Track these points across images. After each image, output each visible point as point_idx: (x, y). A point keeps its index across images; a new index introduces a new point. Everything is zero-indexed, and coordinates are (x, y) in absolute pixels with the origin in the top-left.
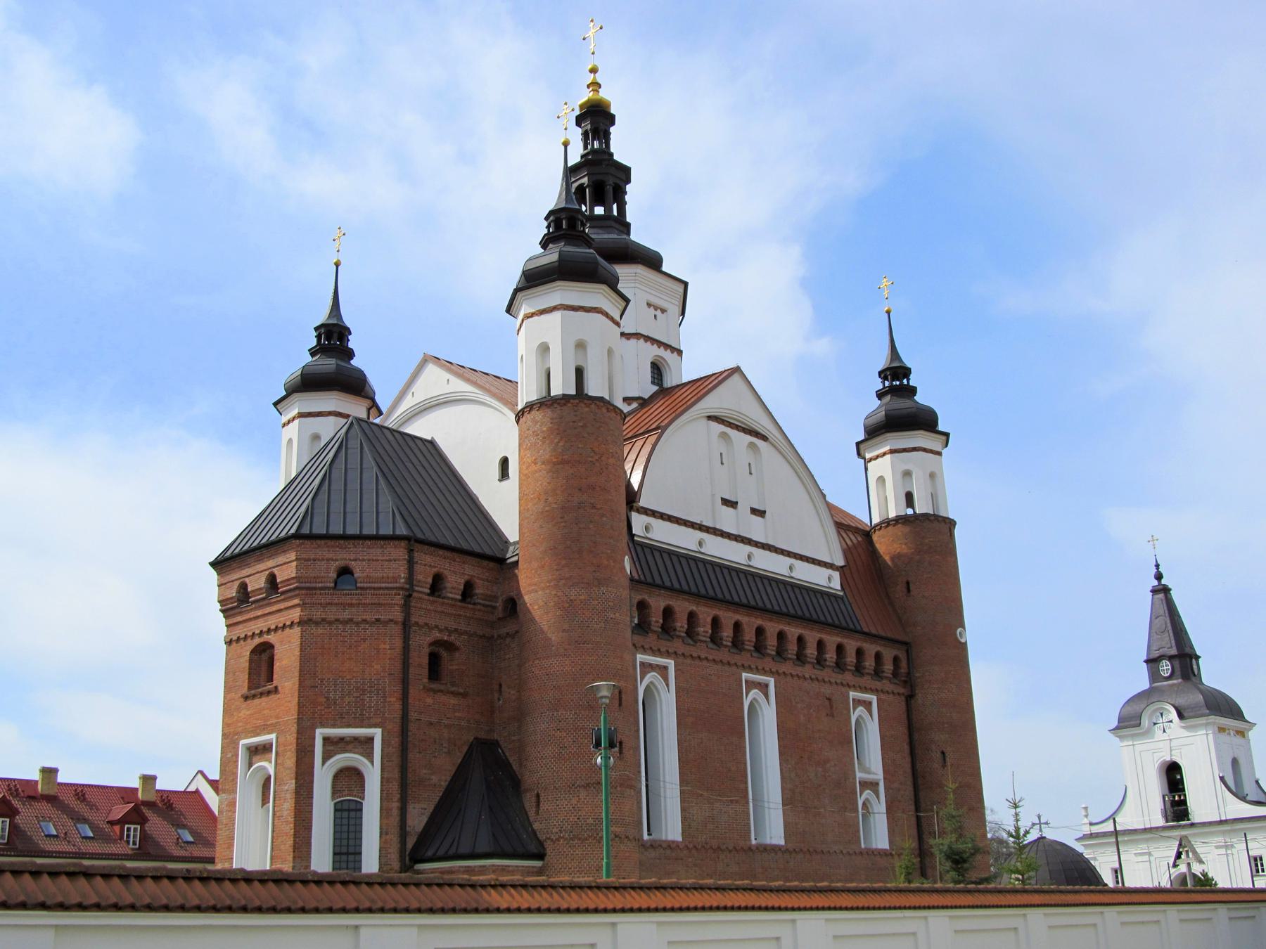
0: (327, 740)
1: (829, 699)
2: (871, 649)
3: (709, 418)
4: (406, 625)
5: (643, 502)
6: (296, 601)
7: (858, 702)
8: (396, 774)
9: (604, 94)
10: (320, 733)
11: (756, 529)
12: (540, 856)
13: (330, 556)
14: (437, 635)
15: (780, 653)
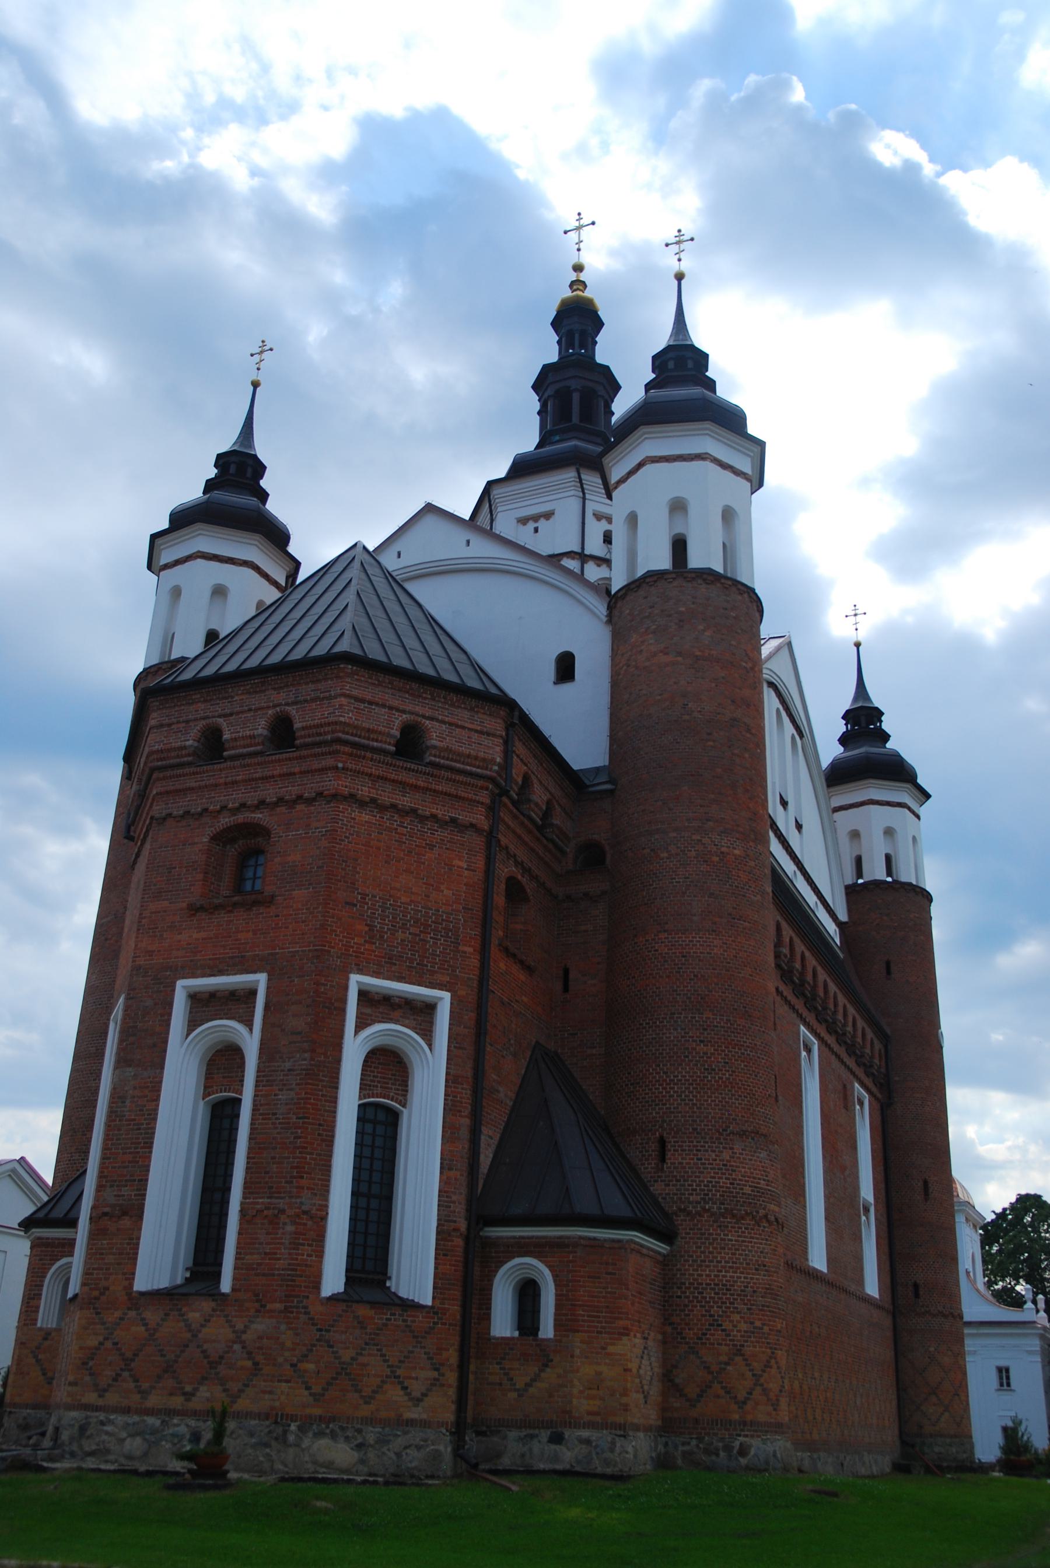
0: (364, 995)
4: (491, 838)
10: (356, 981)
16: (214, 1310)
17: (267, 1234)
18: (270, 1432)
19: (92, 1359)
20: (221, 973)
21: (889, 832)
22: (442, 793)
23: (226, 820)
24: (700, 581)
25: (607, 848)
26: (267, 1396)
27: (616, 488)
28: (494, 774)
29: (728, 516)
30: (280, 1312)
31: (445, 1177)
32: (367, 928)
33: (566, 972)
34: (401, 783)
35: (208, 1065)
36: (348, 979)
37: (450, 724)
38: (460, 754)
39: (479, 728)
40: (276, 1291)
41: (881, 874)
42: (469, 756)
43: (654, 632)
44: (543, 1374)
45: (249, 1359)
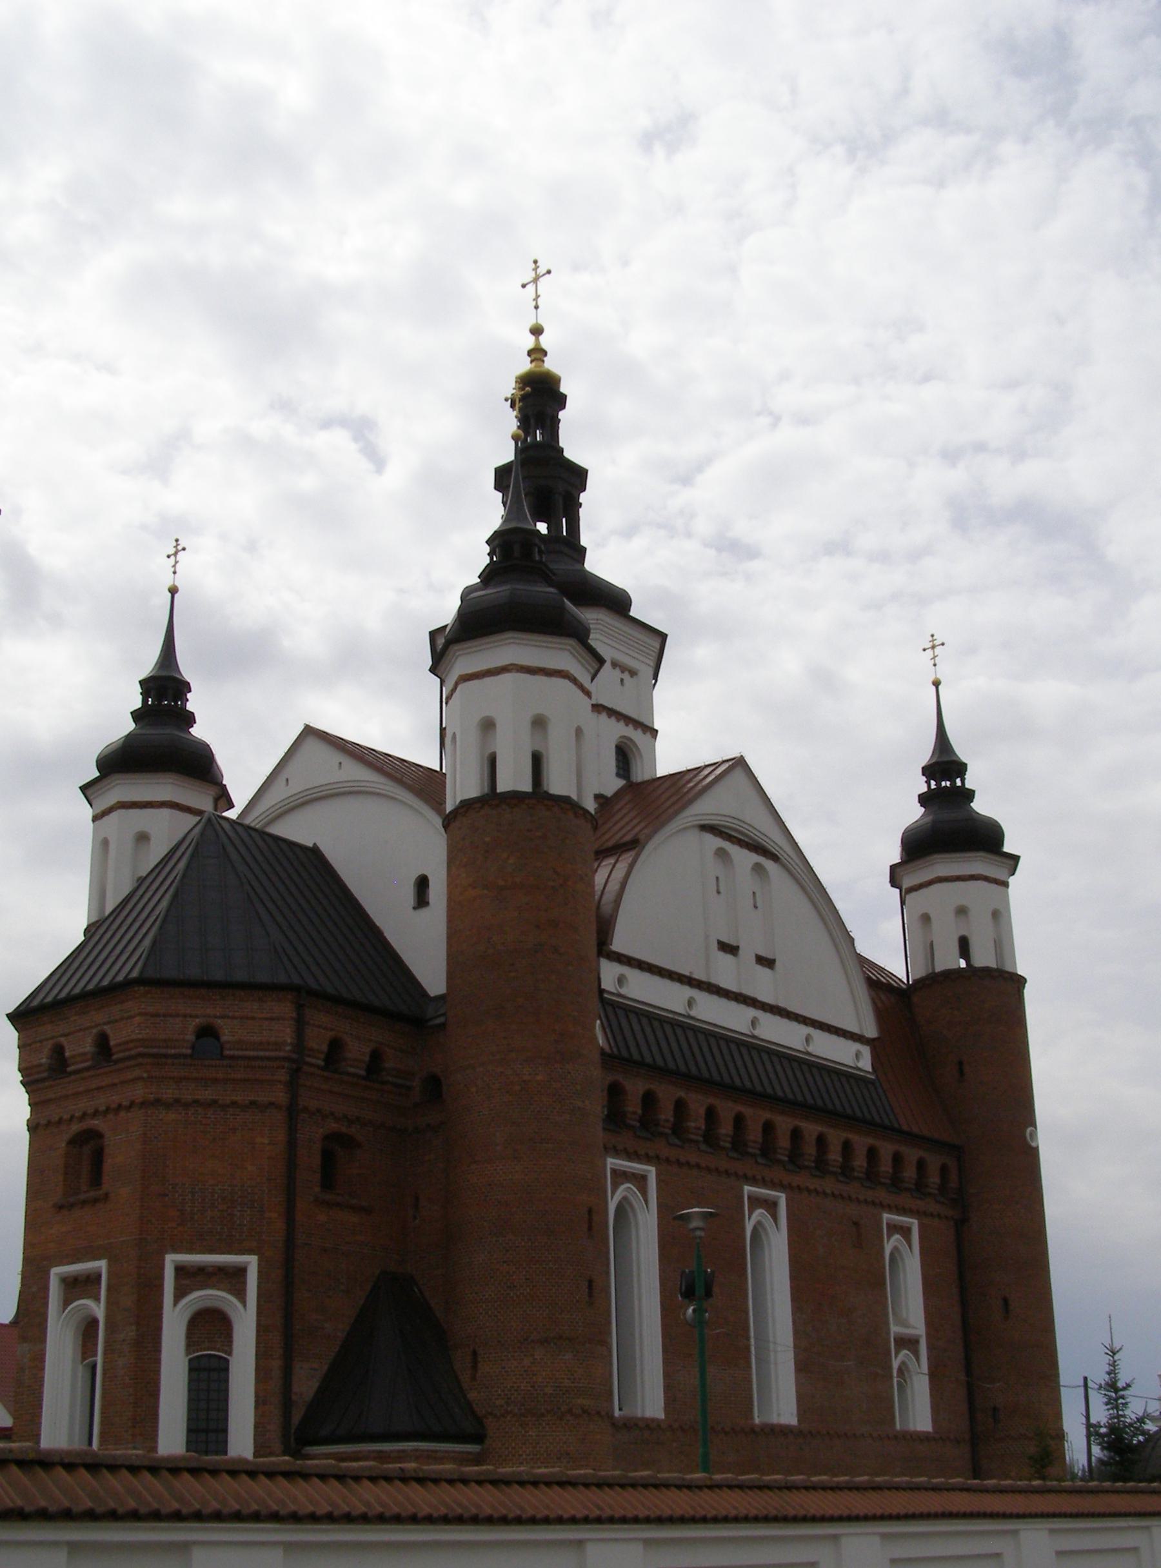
0: (180, 1270)
1: (856, 1224)
2: (912, 1155)
3: (704, 828)
4: (293, 1112)
5: (618, 944)
6: (137, 1072)
7: (894, 1228)
9: (550, 364)
10: (171, 1260)
11: (762, 985)
12: (479, 1438)
14: (334, 1126)
15: (795, 1156)
23: (75, 1128)
24: (504, 806)
36: (164, 1260)
37: (241, 1018)
39: (269, 1015)
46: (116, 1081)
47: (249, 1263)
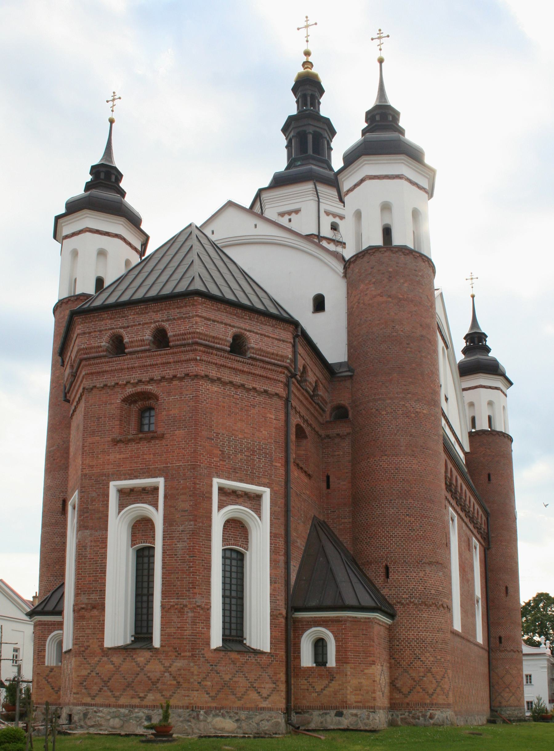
0: (222, 490)
4: (287, 401)
8: (282, 531)
10: (217, 482)
13: (228, 321)
16: (151, 656)
17: (178, 617)
18: (190, 715)
19: (85, 681)
20: (136, 477)
21: (490, 403)
22: (258, 375)
25: (349, 409)
26: (186, 698)
27: (347, 194)
28: (288, 365)
29: (416, 214)
30: (189, 657)
31: (273, 587)
32: (220, 453)
33: (328, 477)
34: (234, 369)
35: (132, 528)
36: (212, 481)
37: (262, 335)
38: (268, 353)
39: (278, 337)
40: (186, 646)
41: (486, 427)
42: (273, 354)
43: (374, 283)
44: (330, 684)
45: (174, 680)
46: (171, 360)
47: (265, 492)
